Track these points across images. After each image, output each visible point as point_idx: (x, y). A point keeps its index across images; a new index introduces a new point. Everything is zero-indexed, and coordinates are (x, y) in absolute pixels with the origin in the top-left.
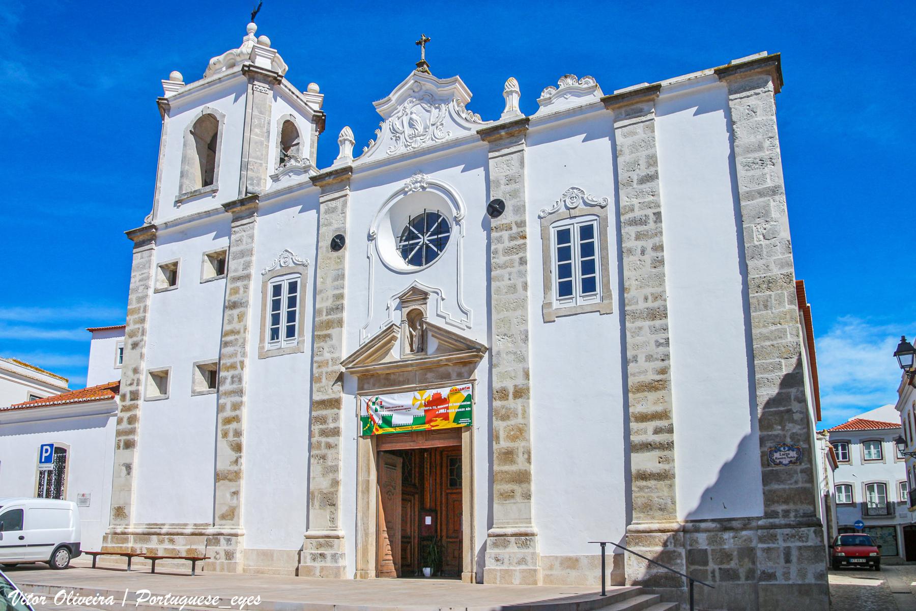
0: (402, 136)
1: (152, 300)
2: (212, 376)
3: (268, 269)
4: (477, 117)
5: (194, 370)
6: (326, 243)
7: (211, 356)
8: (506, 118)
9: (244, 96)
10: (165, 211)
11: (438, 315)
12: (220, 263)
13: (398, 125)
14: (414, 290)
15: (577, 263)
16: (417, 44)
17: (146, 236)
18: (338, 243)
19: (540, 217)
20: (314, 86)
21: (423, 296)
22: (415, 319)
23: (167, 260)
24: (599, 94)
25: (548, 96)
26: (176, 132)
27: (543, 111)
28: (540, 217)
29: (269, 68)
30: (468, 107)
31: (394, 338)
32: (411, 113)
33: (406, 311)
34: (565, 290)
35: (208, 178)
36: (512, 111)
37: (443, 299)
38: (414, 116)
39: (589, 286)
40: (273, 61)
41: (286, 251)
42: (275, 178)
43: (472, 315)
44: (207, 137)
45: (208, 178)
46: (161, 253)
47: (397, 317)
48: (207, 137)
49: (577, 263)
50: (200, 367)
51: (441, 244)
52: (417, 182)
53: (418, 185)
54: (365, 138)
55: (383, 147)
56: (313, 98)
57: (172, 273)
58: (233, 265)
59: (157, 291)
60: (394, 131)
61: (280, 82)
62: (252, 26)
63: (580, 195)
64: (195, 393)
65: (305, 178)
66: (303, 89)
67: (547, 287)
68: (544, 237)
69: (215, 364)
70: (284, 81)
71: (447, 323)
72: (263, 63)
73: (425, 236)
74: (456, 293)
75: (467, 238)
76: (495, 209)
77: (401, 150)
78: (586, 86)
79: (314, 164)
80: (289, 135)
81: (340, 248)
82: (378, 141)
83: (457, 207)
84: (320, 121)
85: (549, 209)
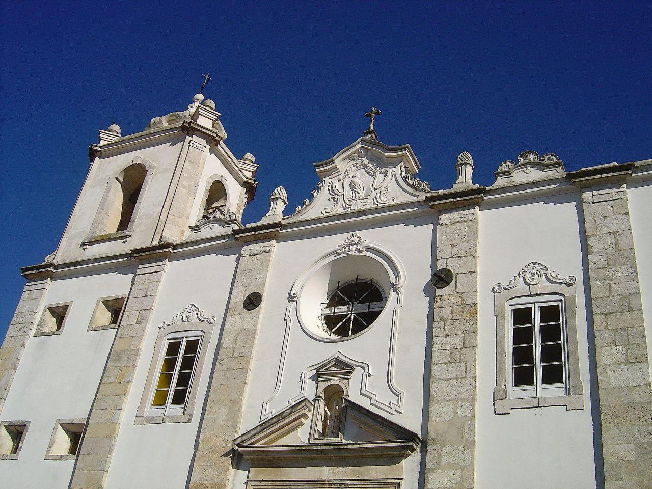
0: (341, 198)
1: (31, 341)
2: (76, 434)
3: (167, 322)
4: (425, 185)
5: (97, 305)
6: (240, 296)
7: (79, 414)
8: (458, 187)
9: (180, 144)
10: (68, 249)
11: (361, 394)
12: (116, 308)
13: (338, 186)
14: (339, 363)
15: (539, 346)
16: (368, 115)
17: (41, 272)
18: (253, 302)
19: (493, 291)
20: (249, 156)
21: (345, 367)
22: (334, 395)
23: (58, 301)
24: (564, 174)
25: (506, 169)
26: (104, 175)
27: (500, 182)
28: (493, 291)
29: (210, 127)
30: (415, 176)
31: (302, 424)
32: (354, 177)
33: (323, 385)
34: (523, 377)
35: (125, 222)
36: (466, 177)
37: (370, 376)
38: (356, 180)
39: (553, 375)
40: (213, 124)
41: (193, 305)
42: (195, 228)
43: (404, 397)
44: (133, 183)
45: (125, 222)
46: (53, 291)
47: (310, 390)
48: (133, 183)
49: (539, 346)
50: (106, 303)
51: (370, 317)
52: (352, 245)
53: (355, 247)
54: (301, 195)
55: (320, 205)
56: (248, 168)
57: (59, 314)
58: (128, 317)
59: (39, 334)
60: (332, 192)
61: (218, 143)
62: (200, 96)
63: (543, 271)
64: (93, 329)
65: (228, 230)
66: (239, 156)
67: (499, 371)
68: (499, 315)
69: (80, 425)
70: (221, 142)
71: (371, 404)
72: (205, 122)
73: (357, 299)
74: (386, 369)
75: (405, 308)
76: (441, 278)
77: (339, 210)
78: (549, 162)
79: (239, 218)
80: (217, 191)
81: (256, 307)
82: (315, 202)
83: (397, 275)
84: (249, 188)
85: (505, 283)
